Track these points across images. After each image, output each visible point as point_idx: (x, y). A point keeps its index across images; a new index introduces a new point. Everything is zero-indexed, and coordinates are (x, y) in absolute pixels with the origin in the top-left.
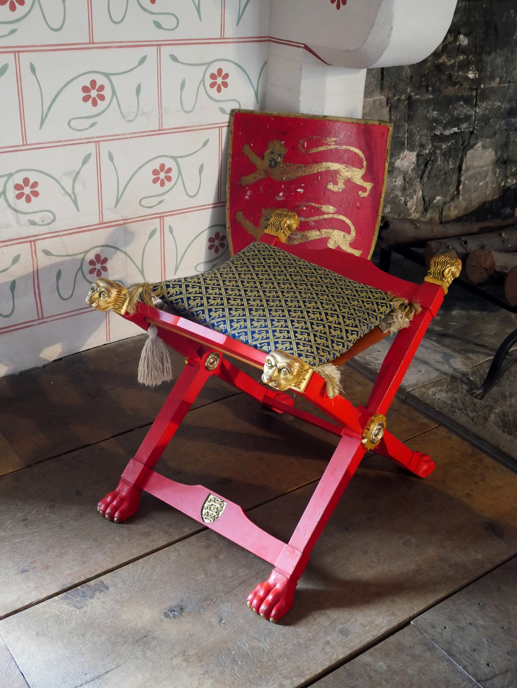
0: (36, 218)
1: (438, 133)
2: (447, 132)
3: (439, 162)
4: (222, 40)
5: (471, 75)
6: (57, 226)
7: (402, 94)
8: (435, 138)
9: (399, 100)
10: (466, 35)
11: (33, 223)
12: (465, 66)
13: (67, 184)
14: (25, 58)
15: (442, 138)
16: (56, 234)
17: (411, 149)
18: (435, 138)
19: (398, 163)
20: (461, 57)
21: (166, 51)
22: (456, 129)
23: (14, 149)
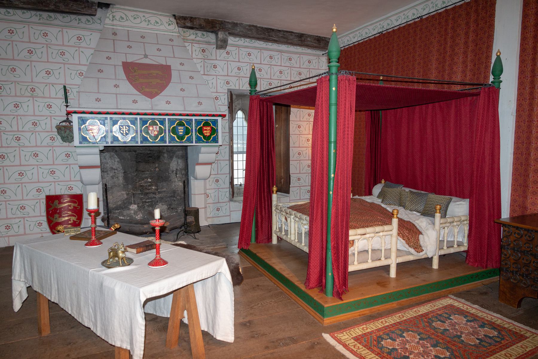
0: (25, 213)
1: (144, 201)
3: (146, 208)
5: (153, 188)
6: (30, 215)
7: (129, 191)
8: (143, 202)
9: (129, 193)
10: (150, 179)
11: (24, 214)
13: (33, 207)
14: (23, 185)
15: (146, 202)
16: (29, 217)
17: (135, 204)
18: (143, 202)
19: (131, 207)
20: (149, 184)
21: (56, 183)
22: (151, 200)
23: (21, 200)
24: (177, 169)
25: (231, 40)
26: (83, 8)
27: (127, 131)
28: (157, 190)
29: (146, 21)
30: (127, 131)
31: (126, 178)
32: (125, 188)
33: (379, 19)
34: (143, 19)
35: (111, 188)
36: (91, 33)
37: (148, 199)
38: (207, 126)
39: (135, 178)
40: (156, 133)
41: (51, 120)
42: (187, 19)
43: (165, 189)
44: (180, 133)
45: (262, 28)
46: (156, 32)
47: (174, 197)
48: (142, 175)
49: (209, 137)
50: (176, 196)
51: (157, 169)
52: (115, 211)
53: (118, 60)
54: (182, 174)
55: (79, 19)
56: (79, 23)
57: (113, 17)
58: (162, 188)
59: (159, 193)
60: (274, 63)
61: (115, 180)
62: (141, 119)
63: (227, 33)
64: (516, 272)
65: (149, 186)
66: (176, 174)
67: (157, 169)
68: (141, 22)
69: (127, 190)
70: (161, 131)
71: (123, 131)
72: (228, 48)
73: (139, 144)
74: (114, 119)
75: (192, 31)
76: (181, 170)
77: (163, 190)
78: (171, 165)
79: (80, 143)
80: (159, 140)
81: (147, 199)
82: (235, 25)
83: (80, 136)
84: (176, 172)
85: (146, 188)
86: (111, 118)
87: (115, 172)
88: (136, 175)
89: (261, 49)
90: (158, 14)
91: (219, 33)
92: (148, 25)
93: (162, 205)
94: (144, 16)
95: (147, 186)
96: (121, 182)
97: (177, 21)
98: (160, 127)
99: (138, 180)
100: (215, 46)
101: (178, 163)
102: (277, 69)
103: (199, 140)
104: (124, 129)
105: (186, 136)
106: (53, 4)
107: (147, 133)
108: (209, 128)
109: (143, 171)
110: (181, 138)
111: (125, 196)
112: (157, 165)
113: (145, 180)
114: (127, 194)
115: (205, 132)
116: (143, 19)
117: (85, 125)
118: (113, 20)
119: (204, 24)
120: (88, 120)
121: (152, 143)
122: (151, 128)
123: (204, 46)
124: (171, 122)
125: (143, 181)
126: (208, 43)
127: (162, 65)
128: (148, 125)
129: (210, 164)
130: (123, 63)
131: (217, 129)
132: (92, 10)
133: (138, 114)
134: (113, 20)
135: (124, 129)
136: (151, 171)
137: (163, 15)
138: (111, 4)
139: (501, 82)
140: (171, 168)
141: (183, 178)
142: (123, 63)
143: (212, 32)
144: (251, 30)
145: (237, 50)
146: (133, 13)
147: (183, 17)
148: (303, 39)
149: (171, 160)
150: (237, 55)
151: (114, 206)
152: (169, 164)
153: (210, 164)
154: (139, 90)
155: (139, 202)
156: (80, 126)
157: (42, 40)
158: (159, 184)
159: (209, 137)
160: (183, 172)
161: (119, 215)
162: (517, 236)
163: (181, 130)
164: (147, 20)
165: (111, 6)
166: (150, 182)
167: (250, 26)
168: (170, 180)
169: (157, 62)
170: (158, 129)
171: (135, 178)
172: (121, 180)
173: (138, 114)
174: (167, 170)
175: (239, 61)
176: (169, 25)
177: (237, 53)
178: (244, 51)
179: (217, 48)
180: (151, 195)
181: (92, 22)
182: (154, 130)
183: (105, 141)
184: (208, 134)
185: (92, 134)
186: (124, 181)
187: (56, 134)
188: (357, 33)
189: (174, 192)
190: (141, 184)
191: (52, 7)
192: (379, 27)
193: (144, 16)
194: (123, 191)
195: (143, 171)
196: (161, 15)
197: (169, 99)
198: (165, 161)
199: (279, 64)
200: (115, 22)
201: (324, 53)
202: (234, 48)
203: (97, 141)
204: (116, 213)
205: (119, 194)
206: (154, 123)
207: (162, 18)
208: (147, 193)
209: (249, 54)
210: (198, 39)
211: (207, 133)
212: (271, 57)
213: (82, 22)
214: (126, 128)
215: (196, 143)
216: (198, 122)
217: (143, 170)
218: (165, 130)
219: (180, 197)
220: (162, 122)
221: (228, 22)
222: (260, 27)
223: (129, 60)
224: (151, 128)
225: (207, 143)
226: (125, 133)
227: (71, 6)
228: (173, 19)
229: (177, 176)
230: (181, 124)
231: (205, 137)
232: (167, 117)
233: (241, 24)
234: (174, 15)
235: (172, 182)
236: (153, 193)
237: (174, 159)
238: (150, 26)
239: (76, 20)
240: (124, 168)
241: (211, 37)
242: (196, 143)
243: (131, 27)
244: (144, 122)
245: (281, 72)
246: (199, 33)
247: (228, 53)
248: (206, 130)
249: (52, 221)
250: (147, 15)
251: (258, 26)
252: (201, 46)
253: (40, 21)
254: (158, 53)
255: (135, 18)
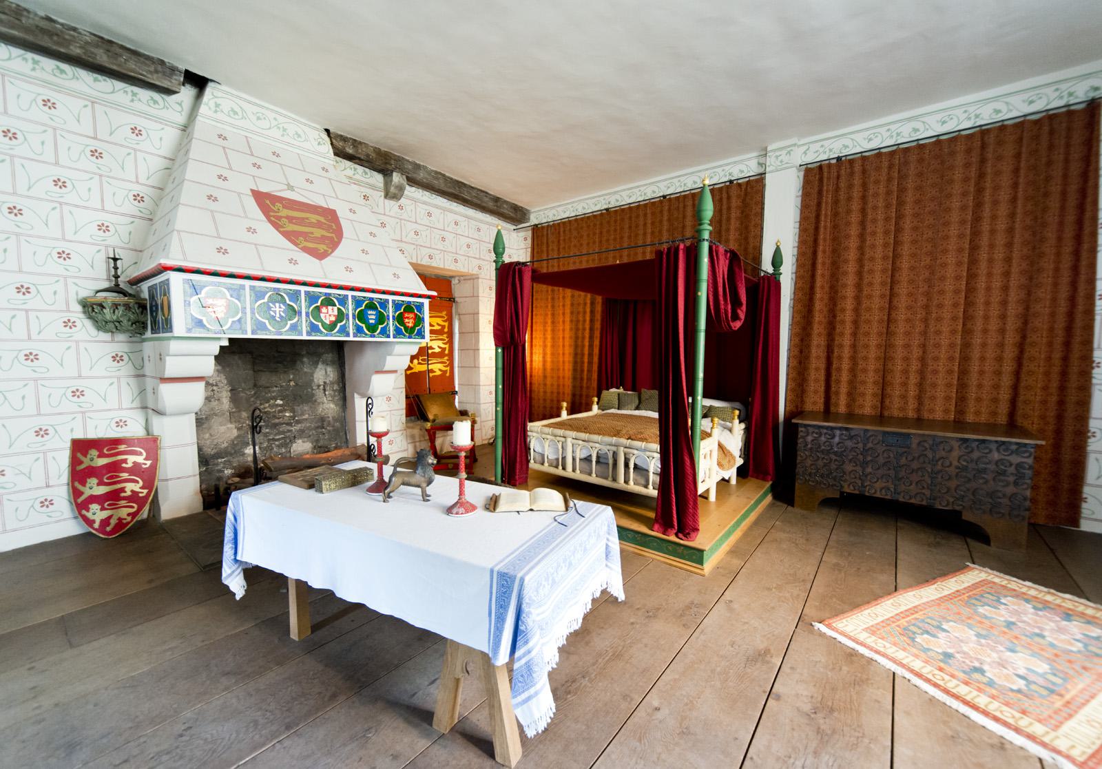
1: (271, 438)
2: (277, 437)
4: (120, 409)
5: (287, 414)
8: (269, 440)
10: (281, 400)
12: (285, 411)
15: (274, 440)
18: (269, 440)
24: (325, 383)
25: (410, 191)
26: (151, 72)
27: (283, 314)
28: (293, 417)
29: (279, 128)
30: (283, 314)
31: (234, 399)
32: (232, 417)
33: (599, 193)
34: (274, 123)
35: (206, 418)
36: (163, 126)
37: (279, 433)
38: (409, 312)
39: (252, 399)
40: (333, 319)
41: (66, 285)
42: (349, 141)
43: (306, 416)
44: (371, 321)
45: (452, 179)
46: (300, 152)
47: (323, 428)
48: (266, 393)
49: (413, 328)
50: (325, 425)
51: (292, 383)
52: (216, 461)
53: (245, 186)
54: (333, 390)
55: (132, 91)
56: (132, 101)
57: (217, 105)
58: (303, 414)
59: (298, 422)
60: (459, 232)
61: (214, 403)
62: (307, 293)
63: (404, 177)
64: (828, 475)
65: (280, 411)
66: (325, 390)
67: (292, 383)
68: (270, 128)
69: (239, 421)
70: (341, 316)
71: (275, 312)
72: (403, 201)
73: (305, 337)
74: (258, 289)
75: (348, 163)
76: (332, 383)
77: (304, 417)
78: (315, 376)
79: (189, 330)
80: (337, 332)
81: (275, 435)
82: (417, 167)
83: (189, 317)
84: (324, 386)
85: (274, 417)
86: (252, 288)
87: (213, 390)
88: (255, 394)
89: (444, 209)
90: (301, 123)
91: (394, 174)
92: (283, 135)
93: (303, 442)
94: (275, 119)
95: (275, 412)
96: (227, 407)
97: (331, 141)
98: (339, 309)
99: (258, 402)
100: (383, 194)
101: (326, 372)
102: (464, 241)
103: (398, 333)
104: (278, 309)
105: (380, 326)
106: (78, 45)
107: (318, 318)
108: (412, 315)
109: (268, 387)
110: (372, 329)
111: (235, 433)
112: (291, 377)
113: (272, 402)
114: (239, 429)
115: (407, 320)
116: (274, 123)
117: (199, 296)
118: (216, 111)
119: (373, 155)
120: (205, 287)
121: (327, 335)
122: (324, 310)
123: (369, 192)
124: (358, 303)
125: (267, 405)
126: (373, 187)
127: (321, 207)
128: (319, 304)
129: (395, 372)
130: (253, 191)
131: (423, 318)
132: (171, 82)
133: (305, 284)
134: (216, 111)
135: (278, 309)
136: (281, 386)
137: (309, 126)
138: (212, 81)
139: (781, 274)
140: (315, 380)
141: (335, 396)
142: (253, 191)
143: (379, 171)
144: (437, 179)
145: (413, 206)
146: (256, 109)
147: (341, 136)
148: (499, 204)
149: (316, 368)
150: (414, 212)
151: (215, 451)
152: (312, 375)
153: (395, 372)
154: (296, 244)
155: (262, 441)
156: (188, 299)
157: (40, 113)
158: (296, 407)
159: (413, 328)
160: (336, 387)
161: (224, 468)
162: (815, 435)
163: (372, 316)
164: (281, 126)
165: (210, 85)
166: (280, 405)
167: (436, 173)
168: (316, 401)
169: (312, 201)
170: (336, 312)
171: (252, 399)
172: (226, 403)
173: (305, 284)
174: (309, 383)
175: (416, 223)
176: (319, 144)
177: (414, 210)
178: (422, 209)
179: (386, 196)
180: (284, 428)
181: (162, 106)
182: (329, 314)
183: (241, 329)
184: (410, 325)
185: (214, 316)
186: (232, 406)
187: (82, 316)
188: (570, 206)
189: (322, 419)
190: (265, 408)
191: (76, 51)
192: (603, 202)
193: (275, 119)
194: (231, 422)
195: (268, 387)
196: (305, 125)
197: (351, 264)
198: (305, 370)
199: (466, 234)
200: (219, 116)
201: (515, 227)
202: (409, 202)
203: (224, 328)
204: (217, 464)
205: (223, 429)
206: (328, 302)
207: (307, 129)
208: (275, 425)
209: (429, 214)
210: (357, 177)
211: (410, 323)
212: (456, 223)
213: (140, 100)
214: (280, 307)
215: (394, 337)
216: (397, 306)
217: (268, 385)
218: (348, 315)
219: (333, 426)
220: (343, 301)
221: (408, 161)
222: (449, 178)
223: (264, 189)
224: (324, 310)
225: (410, 337)
226: (278, 315)
227: (123, 60)
228: (325, 136)
229: (327, 393)
230: (371, 306)
231: (406, 328)
232: (350, 293)
233: (425, 168)
234: (327, 131)
235: (319, 404)
236: (287, 424)
237: (320, 366)
238: (286, 139)
239: (126, 92)
240: (230, 383)
241: (378, 179)
242: (394, 337)
243: (252, 132)
244: (312, 298)
245: (468, 246)
246: (360, 169)
247: (401, 207)
248: (408, 318)
249: (82, 493)
250: (281, 119)
251: (447, 174)
252: (363, 189)
253: (33, 73)
254: (308, 186)
255: (258, 118)
